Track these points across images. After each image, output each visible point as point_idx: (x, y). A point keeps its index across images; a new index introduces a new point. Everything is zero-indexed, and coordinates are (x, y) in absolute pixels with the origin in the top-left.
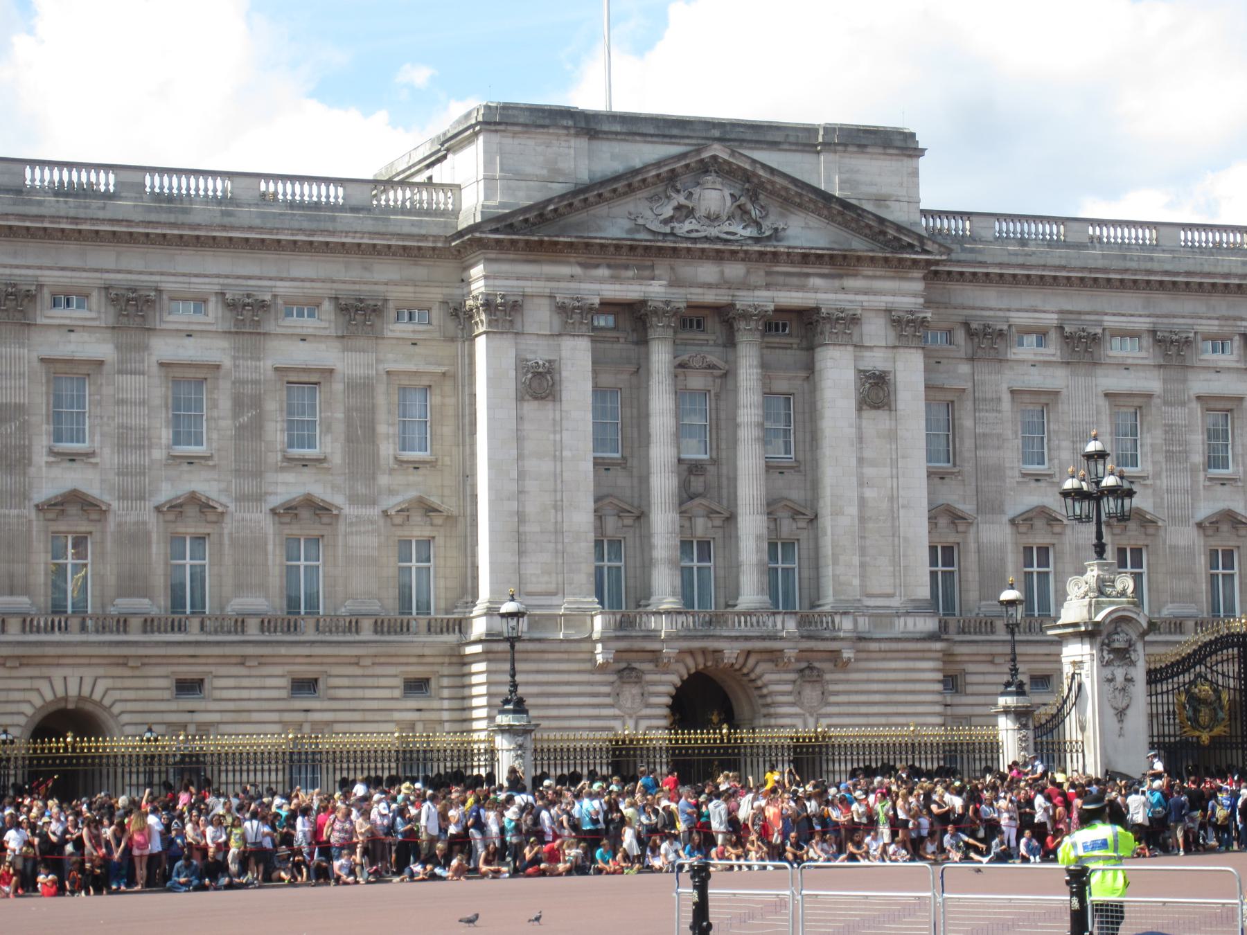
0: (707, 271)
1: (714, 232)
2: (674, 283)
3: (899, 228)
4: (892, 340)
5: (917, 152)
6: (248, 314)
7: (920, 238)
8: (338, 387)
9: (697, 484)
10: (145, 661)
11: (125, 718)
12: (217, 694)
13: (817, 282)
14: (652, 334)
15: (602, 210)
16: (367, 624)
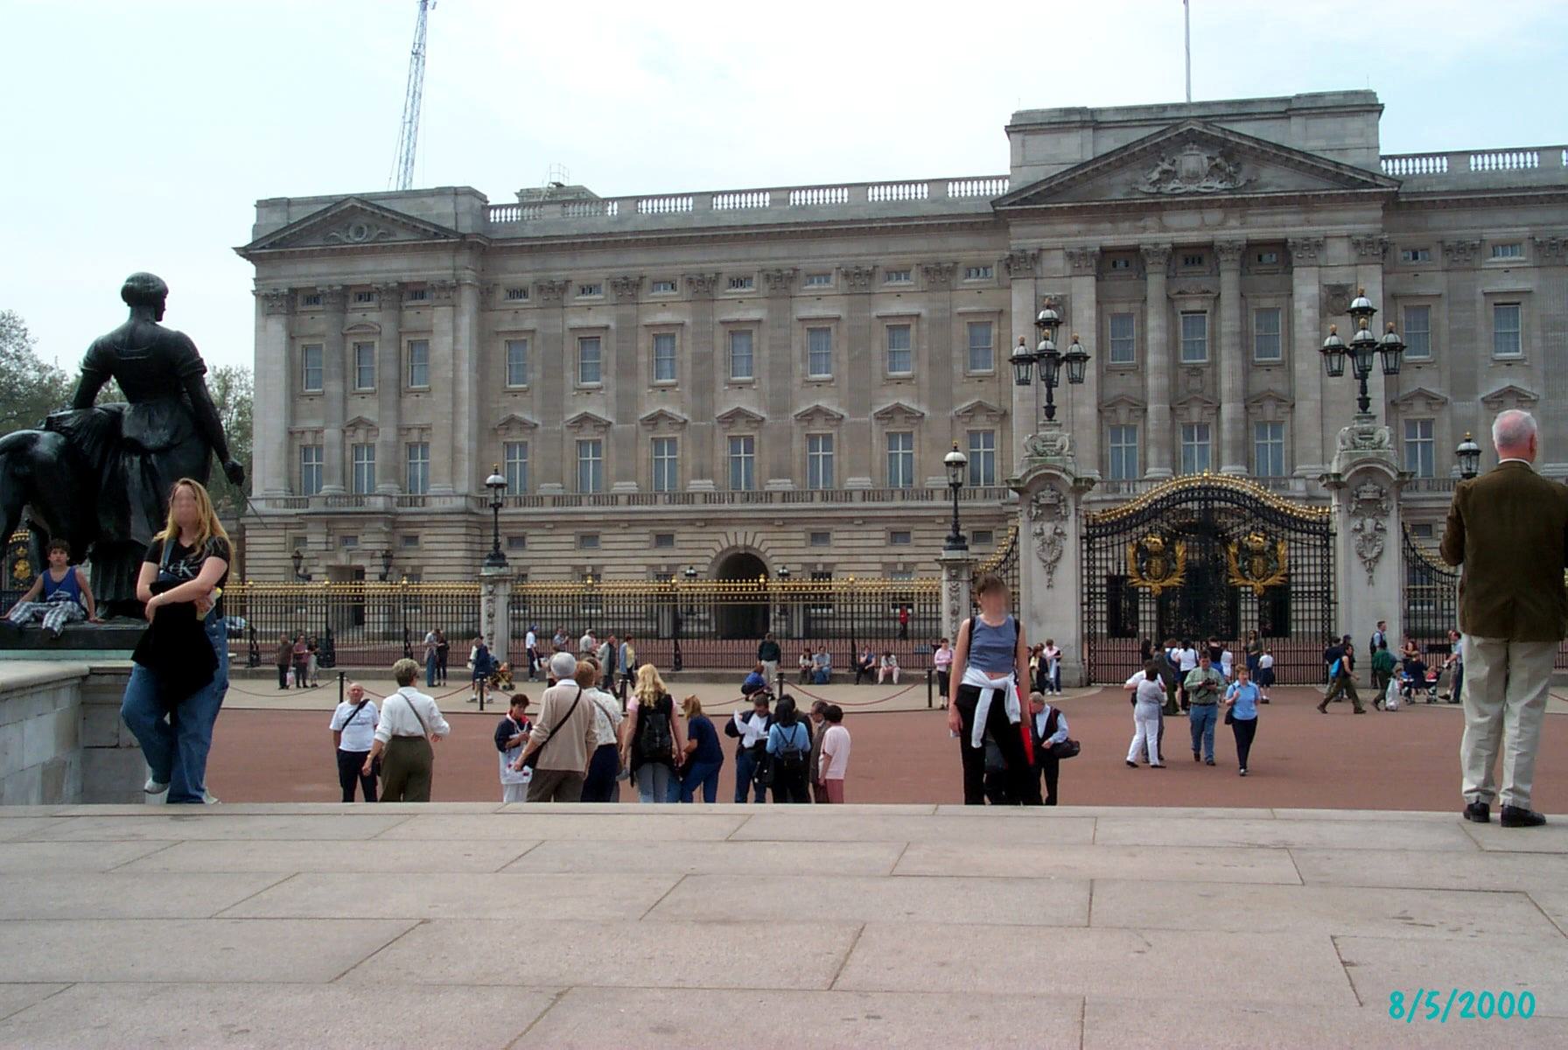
0: (1190, 219)
1: (1192, 188)
2: (1164, 229)
3: (1352, 168)
4: (1353, 257)
5: (1379, 109)
6: (860, 279)
7: (1373, 175)
8: (924, 326)
9: (1195, 383)
10: (787, 522)
11: (775, 559)
12: (836, 543)
13: (1288, 218)
14: (1149, 269)
15: (1103, 181)
16: (937, 493)
